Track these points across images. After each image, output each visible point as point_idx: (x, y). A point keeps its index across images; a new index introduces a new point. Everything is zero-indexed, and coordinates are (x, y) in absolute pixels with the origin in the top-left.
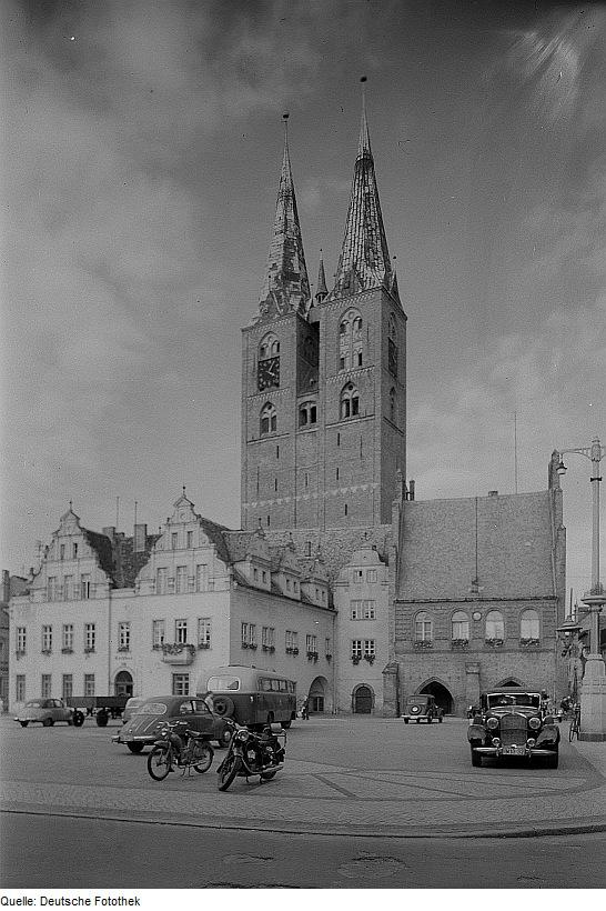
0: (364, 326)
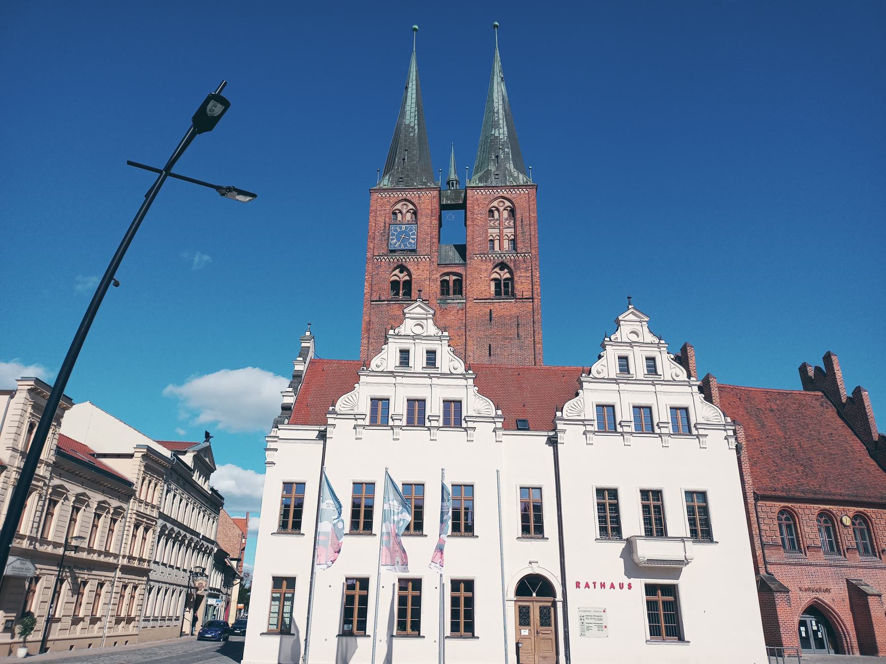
0: (518, 216)
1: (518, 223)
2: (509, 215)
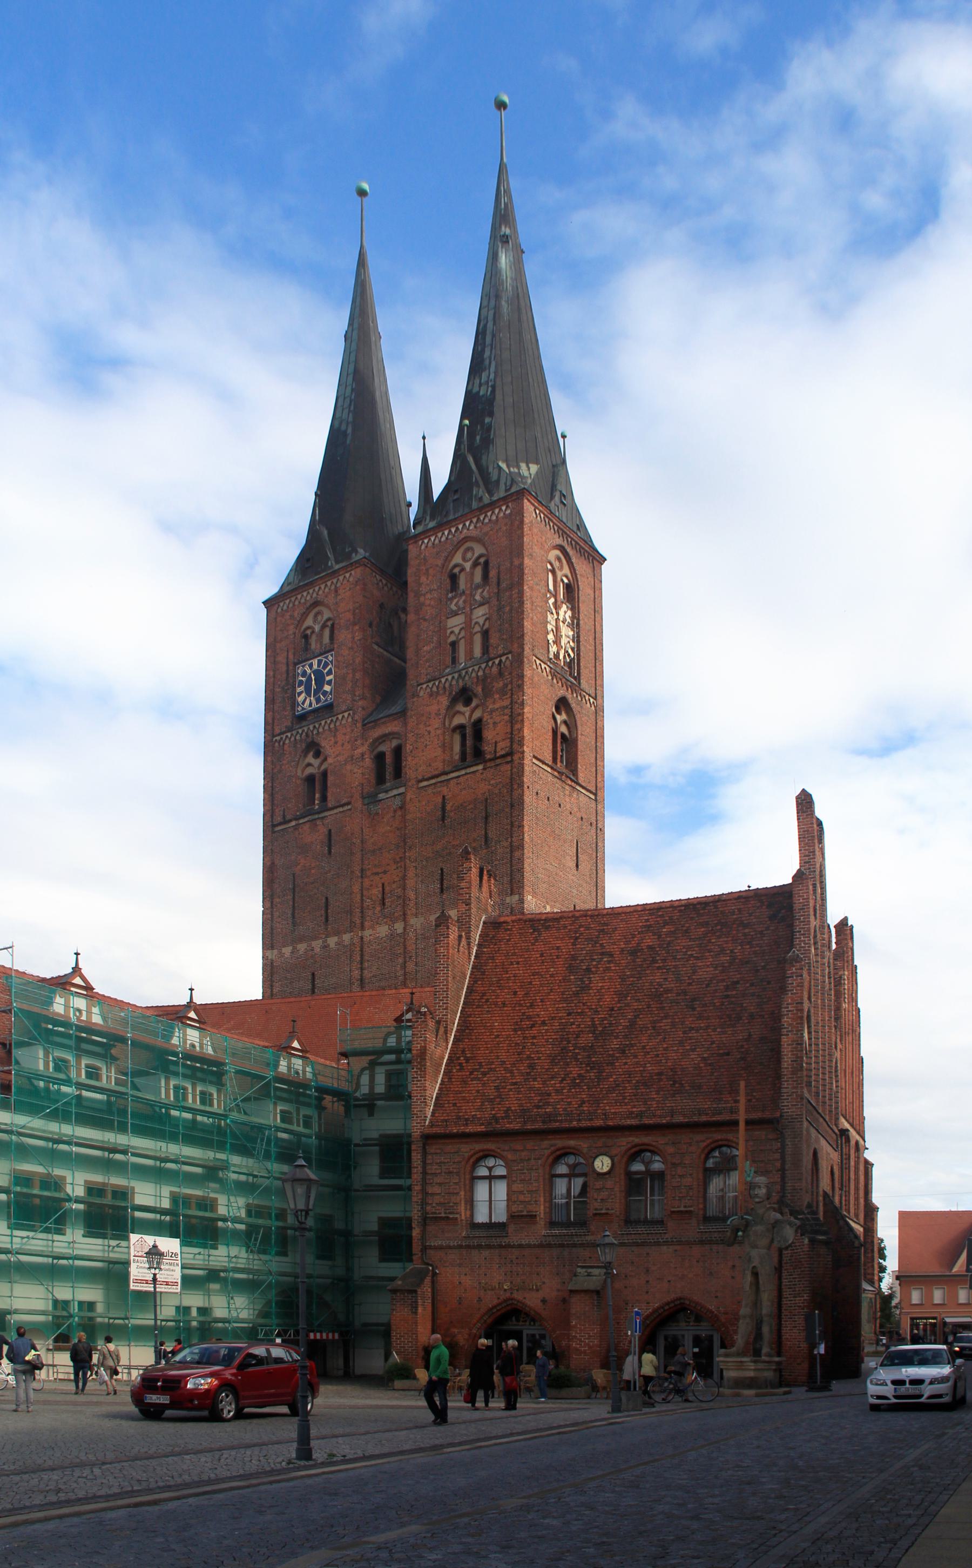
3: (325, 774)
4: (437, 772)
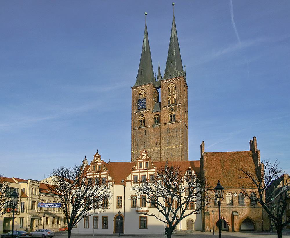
0: (177, 89)
1: (177, 92)
2: (175, 90)
3: (144, 120)
4: (166, 122)
